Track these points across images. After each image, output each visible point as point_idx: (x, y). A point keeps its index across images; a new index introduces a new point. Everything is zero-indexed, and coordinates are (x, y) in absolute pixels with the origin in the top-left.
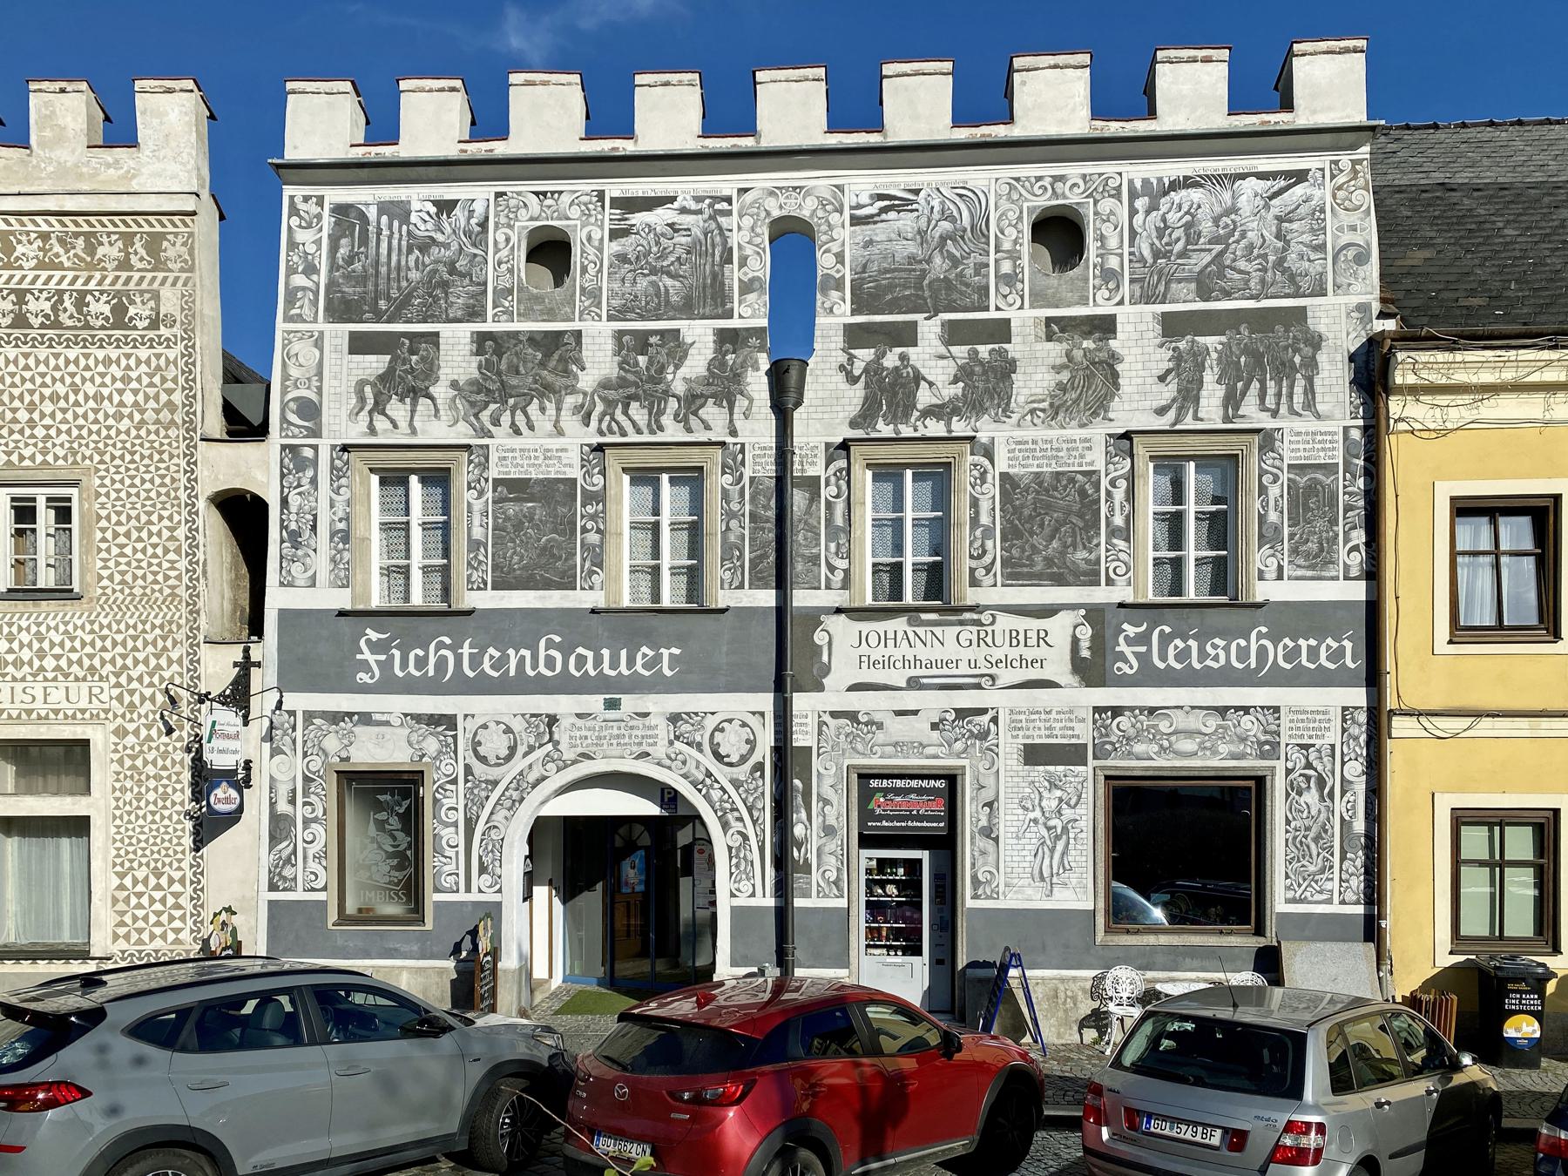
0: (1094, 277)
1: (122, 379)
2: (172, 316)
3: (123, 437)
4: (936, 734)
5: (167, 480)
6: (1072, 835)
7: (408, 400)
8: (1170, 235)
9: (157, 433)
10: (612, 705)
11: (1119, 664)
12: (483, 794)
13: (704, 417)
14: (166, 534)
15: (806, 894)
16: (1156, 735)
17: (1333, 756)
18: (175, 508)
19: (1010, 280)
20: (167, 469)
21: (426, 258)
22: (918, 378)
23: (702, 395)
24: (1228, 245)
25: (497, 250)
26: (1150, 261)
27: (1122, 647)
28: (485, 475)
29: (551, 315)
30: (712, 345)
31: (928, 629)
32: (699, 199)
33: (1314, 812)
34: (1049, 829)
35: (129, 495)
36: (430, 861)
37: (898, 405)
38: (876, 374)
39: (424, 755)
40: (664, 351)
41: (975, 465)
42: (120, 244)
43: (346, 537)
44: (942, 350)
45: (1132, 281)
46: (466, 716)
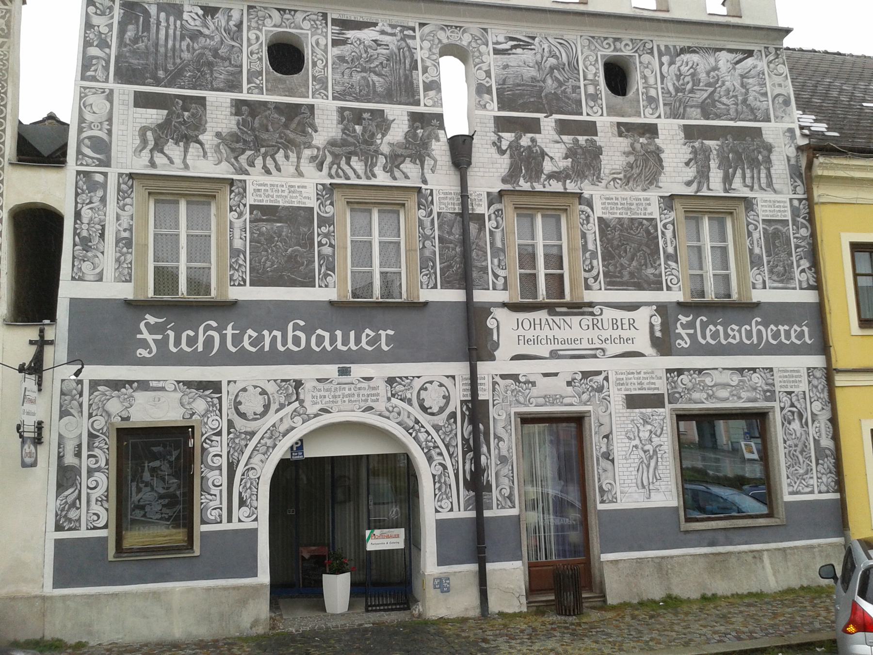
0: (643, 101)
4: (570, 389)
6: (659, 456)
7: (181, 144)
8: (683, 79)
10: (344, 372)
11: (679, 341)
12: (243, 443)
13: (405, 170)
15: (490, 508)
16: (705, 388)
17: (805, 398)
19: (594, 97)
21: (195, 45)
22: (543, 154)
23: (402, 155)
24: (716, 88)
25: (250, 44)
26: (674, 93)
27: (680, 330)
28: (243, 202)
29: (291, 93)
30: (407, 122)
31: (561, 317)
32: (393, 27)
33: (798, 435)
34: (645, 452)
36: (198, 498)
37: (532, 171)
38: (516, 150)
39: (194, 414)
40: (374, 124)
41: (583, 212)
43: (129, 243)
44: (557, 137)
45: (665, 105)
46: (229, 382)
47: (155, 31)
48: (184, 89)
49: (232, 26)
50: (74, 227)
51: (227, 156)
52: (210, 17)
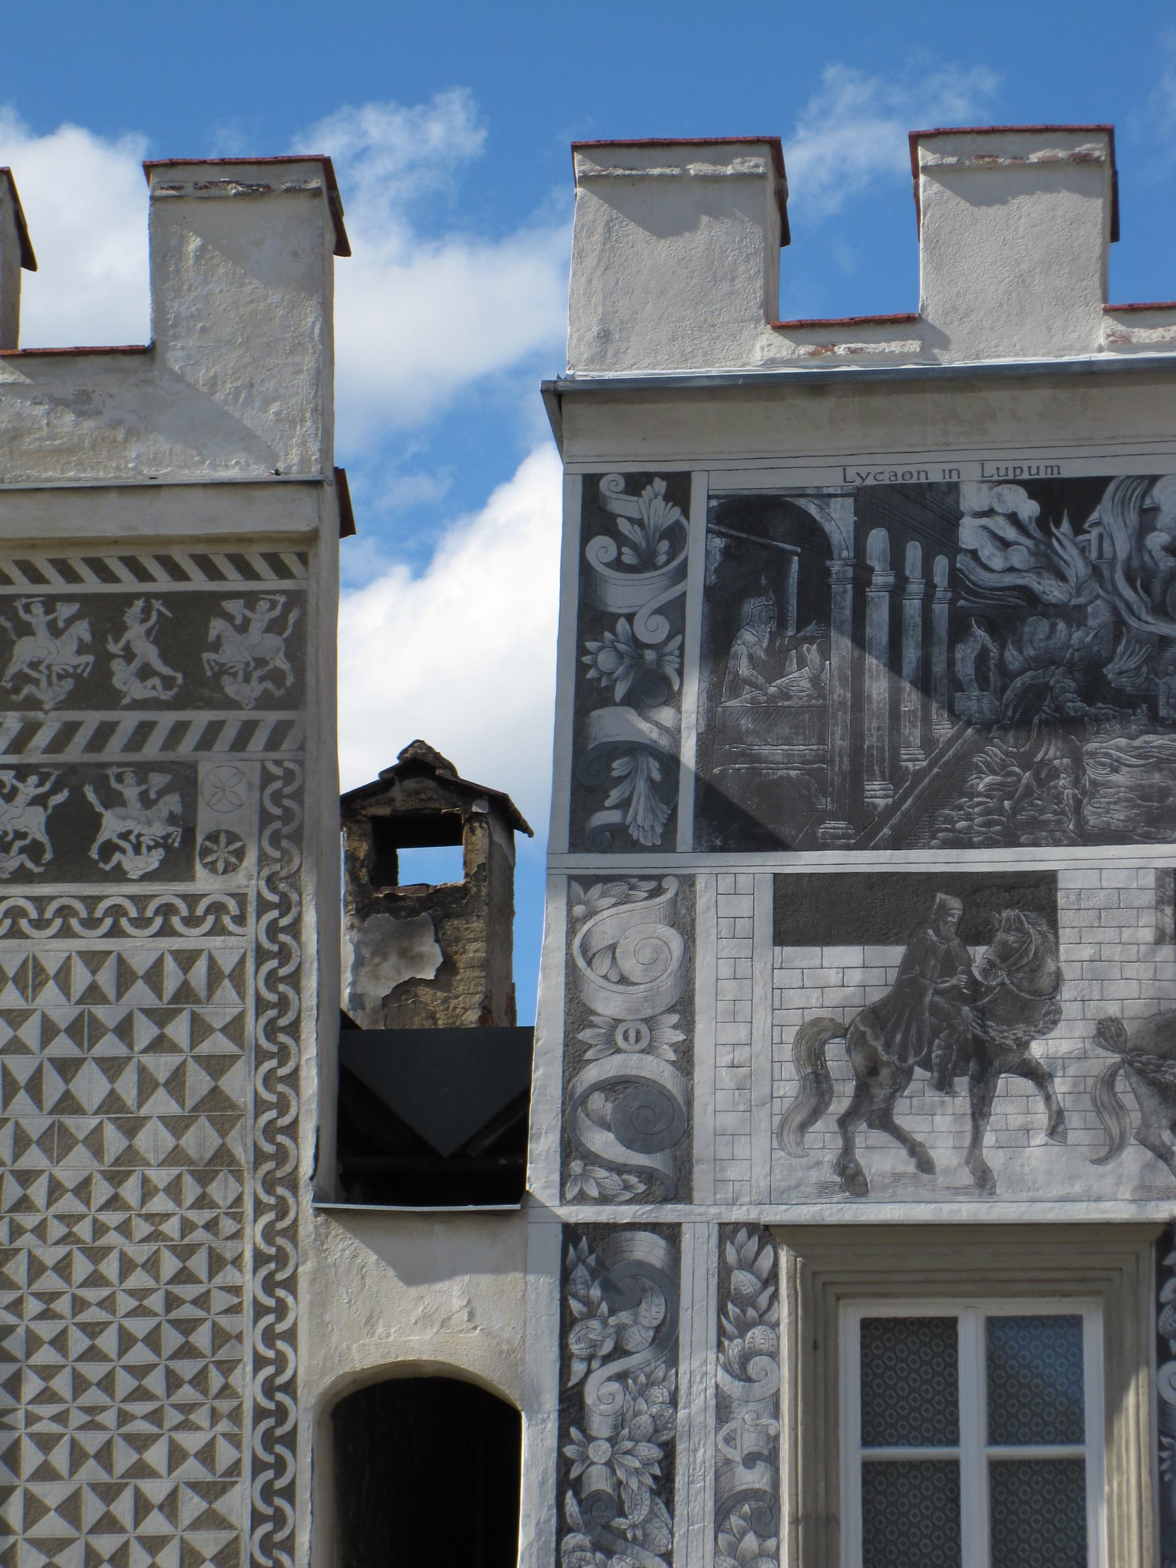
1: (74, 1030)
2: (232, 837)
3: (69, 1204)
5: (202, 1338)
7: (962, 1083)
9: (174, 1190)
14: (192, 1506)
18: (224, 1426)
20: (202, 1301)
35: (80, 1384)
42: (82, 630)
47: (848, 612)
48: (971, 845)
49: (1159, 554)
51: (1146, 1124)
52: (1066, 526)
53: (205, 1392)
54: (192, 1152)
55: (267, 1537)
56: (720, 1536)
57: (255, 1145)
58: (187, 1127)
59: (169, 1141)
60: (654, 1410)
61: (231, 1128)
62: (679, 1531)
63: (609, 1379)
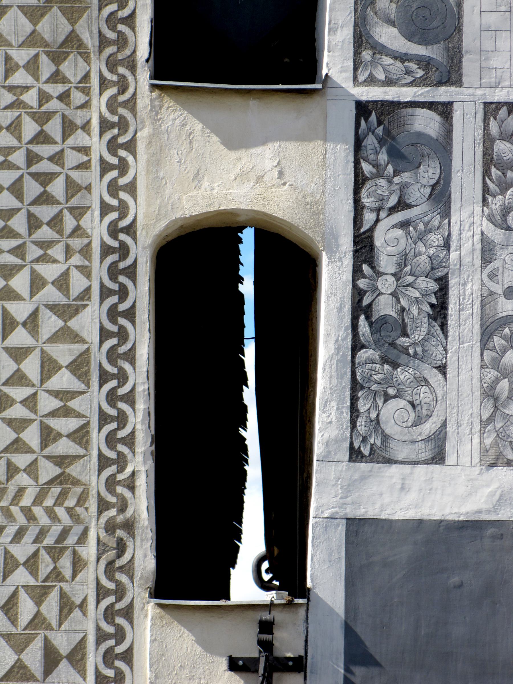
18: (76, 259)
50: (355, 286)
53: (60, 232)
54: (47, 36)
55: (113, 349)
56: (486, 352)
57: (100, 32)
58: (42, 15)
59: (29, 27)
60: (431, 252)
61: (80, 18)
62: (452, 348)
63: (394, 226)
